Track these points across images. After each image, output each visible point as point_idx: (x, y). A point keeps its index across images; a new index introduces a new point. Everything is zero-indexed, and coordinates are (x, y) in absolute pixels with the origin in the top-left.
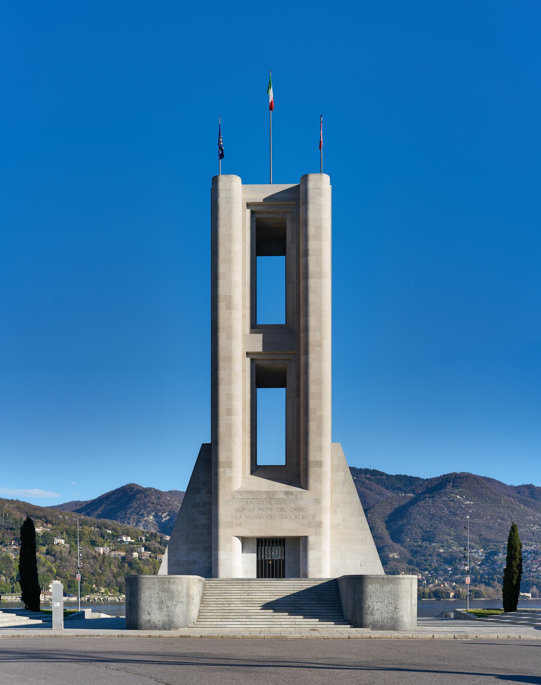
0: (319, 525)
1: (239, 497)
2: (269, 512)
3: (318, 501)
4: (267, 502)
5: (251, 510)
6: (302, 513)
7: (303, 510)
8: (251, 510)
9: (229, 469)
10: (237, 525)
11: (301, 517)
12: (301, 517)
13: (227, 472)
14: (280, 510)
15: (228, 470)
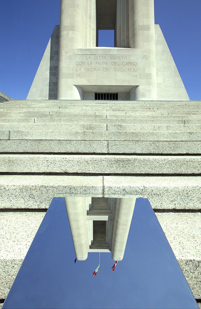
0: (148, 76)
1: (80, 53)
2: (105, 65)
3: (146, 57)
4: (103, 59)
5: (89, 64)
6: (134, 67)
7: (134, 64)
8: (89, 64)
9: (71, 32)
10: (77, 76)
11: (132, 70)
12: (132, 70)
13: (70, 34)
14: (114, 64)
15: (71, 33)
